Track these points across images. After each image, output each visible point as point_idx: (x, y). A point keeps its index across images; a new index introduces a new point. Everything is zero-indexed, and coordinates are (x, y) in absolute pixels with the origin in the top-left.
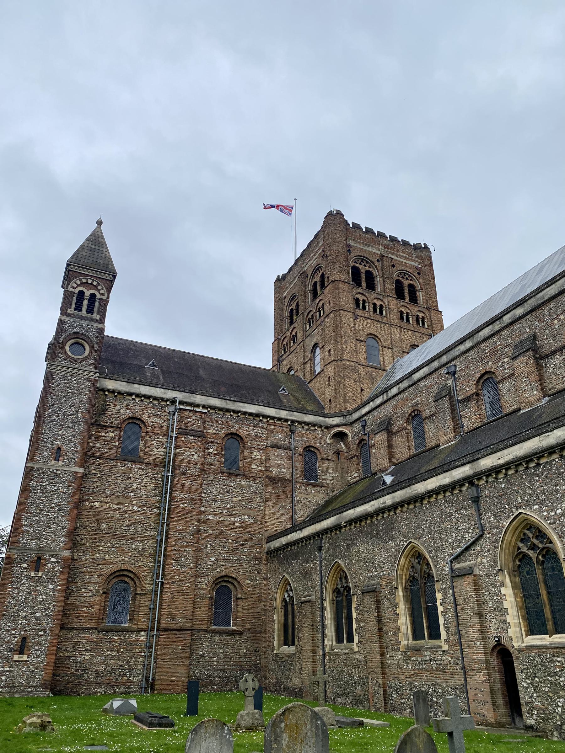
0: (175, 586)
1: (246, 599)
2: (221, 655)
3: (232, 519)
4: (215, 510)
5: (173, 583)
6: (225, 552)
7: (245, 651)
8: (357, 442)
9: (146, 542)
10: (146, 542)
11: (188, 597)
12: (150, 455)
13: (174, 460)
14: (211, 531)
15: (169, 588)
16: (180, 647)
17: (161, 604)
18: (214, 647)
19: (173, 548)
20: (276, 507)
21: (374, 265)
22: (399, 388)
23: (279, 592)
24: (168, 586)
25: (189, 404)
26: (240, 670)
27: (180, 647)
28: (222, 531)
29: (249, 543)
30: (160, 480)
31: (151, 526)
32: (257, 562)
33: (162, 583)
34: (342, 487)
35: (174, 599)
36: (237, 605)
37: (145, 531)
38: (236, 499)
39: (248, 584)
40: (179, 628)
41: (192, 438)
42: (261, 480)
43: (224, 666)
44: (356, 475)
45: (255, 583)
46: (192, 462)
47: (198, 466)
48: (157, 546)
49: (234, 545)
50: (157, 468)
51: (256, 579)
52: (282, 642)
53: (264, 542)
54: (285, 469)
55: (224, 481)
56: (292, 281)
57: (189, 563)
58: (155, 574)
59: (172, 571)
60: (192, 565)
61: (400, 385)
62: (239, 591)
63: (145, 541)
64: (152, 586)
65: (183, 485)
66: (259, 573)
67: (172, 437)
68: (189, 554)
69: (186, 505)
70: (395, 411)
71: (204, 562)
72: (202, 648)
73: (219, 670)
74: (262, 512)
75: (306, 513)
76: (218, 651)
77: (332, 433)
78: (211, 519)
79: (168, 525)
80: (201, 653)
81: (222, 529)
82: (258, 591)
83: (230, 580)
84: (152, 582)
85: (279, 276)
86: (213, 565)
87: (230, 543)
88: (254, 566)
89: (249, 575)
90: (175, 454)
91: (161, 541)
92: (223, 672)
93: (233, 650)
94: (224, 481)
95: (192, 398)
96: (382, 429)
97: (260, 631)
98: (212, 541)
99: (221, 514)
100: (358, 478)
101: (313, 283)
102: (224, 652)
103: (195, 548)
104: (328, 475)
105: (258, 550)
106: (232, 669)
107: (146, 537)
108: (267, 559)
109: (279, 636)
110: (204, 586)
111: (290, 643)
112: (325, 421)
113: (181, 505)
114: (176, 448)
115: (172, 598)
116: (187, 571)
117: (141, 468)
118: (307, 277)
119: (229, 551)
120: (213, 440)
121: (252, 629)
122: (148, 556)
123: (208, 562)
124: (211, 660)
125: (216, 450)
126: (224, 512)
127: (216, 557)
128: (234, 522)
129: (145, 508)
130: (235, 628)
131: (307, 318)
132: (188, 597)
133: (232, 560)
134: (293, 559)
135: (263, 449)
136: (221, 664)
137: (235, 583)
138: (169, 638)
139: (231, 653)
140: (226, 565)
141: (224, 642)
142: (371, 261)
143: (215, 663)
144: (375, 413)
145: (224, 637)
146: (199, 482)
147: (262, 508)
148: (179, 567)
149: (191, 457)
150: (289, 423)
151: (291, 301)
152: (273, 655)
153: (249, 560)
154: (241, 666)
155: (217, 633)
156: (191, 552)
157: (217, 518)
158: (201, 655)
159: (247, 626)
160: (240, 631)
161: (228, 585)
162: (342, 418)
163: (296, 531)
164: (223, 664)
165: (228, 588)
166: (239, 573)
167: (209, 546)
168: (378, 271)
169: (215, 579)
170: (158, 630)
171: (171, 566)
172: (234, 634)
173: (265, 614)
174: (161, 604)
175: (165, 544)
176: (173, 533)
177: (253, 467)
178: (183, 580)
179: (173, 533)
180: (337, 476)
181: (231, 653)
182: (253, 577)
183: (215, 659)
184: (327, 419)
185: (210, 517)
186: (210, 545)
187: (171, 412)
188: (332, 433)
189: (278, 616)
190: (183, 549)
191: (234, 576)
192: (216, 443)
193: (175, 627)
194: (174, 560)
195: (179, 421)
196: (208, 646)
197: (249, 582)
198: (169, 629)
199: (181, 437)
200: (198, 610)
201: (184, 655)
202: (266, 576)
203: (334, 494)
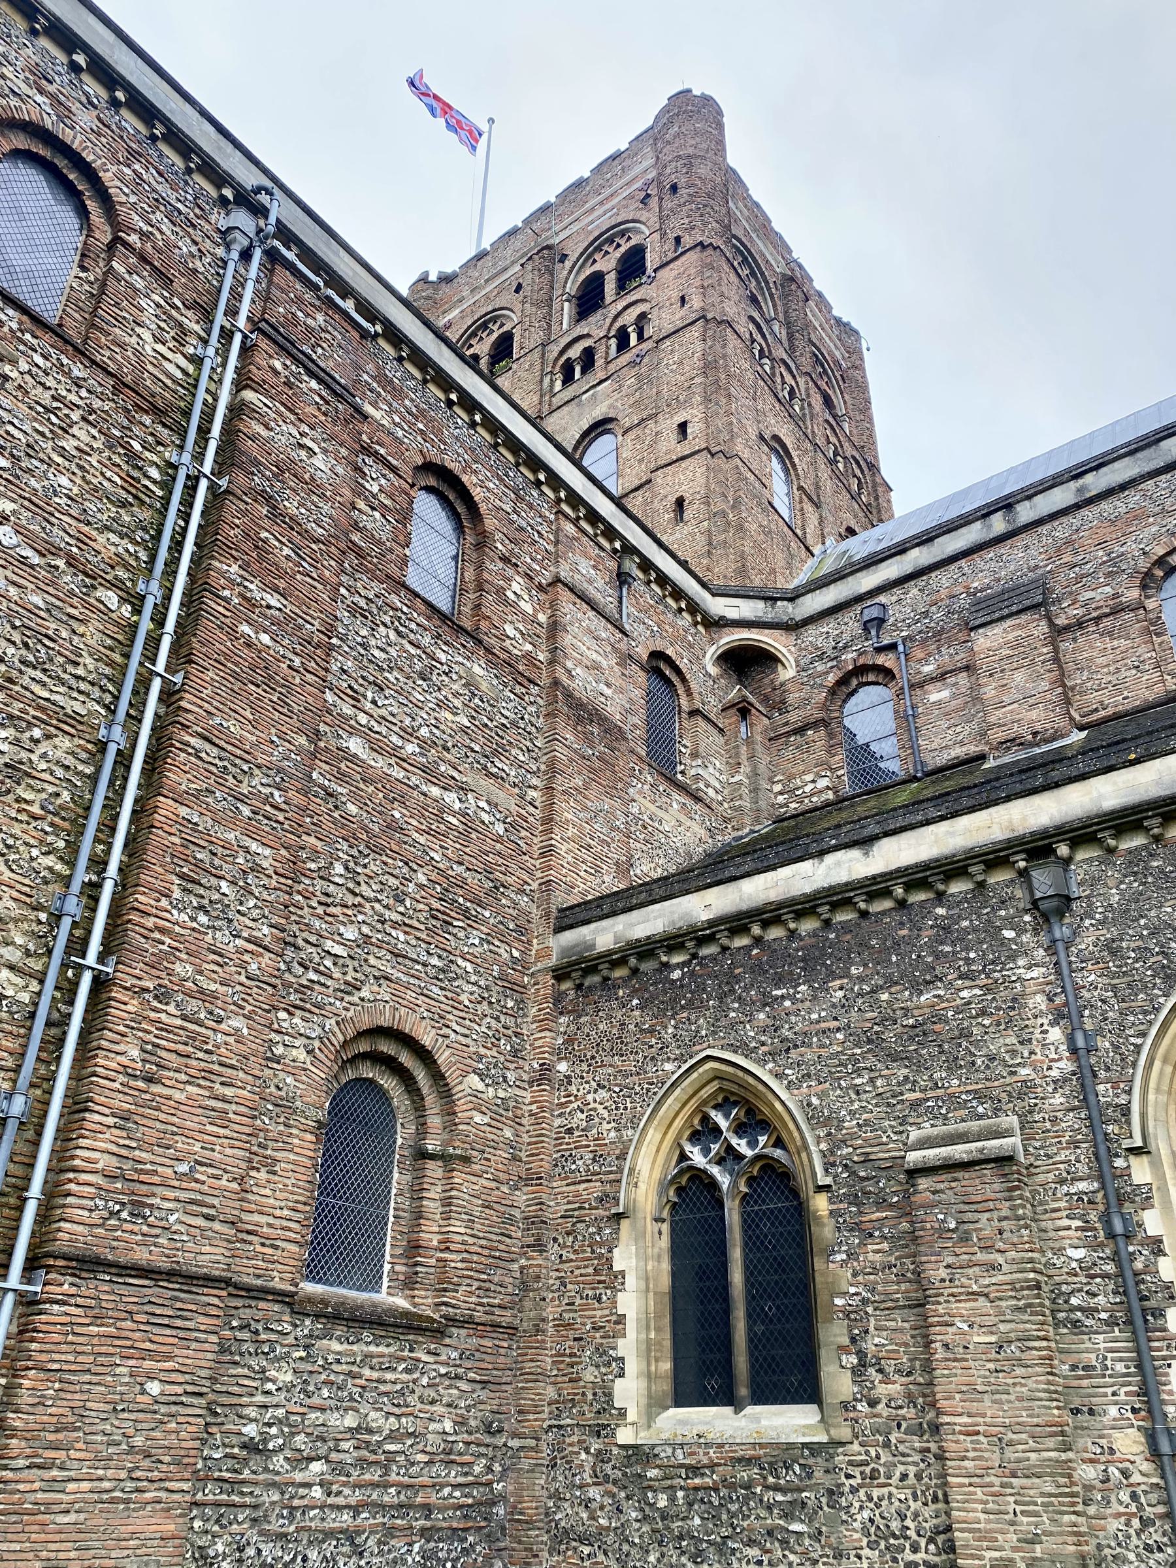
0: (169, 1015)
1: (466, 1160)
2: (345, 1445)
3: (435, 791)
4: (373, 723)
5: (163, 996)
6: (399, 918)
7: (448, 1426)
8: (831, 679)
9: (37, 733)
10: (37, 733)
11: (229, 1092)
12: (122, 346)
13: (229, 431)
14: (352, 809)
15: (139, 1018)
16: (154, 1388)
17: (77, 1106)
18: (316, 1400)
19: (184, 811)
20: (585, 808)
21: (769, 289)
22: (1080, 490)
23: (653, 1135)
24: (133, 1006)
25: (307, 254)
26: (423, 1531)
27: (154, 1388)
28: (393, 827)
29: (487, 914)
30: (154, 473)
31: (76, 664)
32: (510, 1004)
33: (100, 984)
34: (757, 820)
35: (156, 1089)
36: (416, 1191)
37: (38, 674)
38: (450, 717)
39: (476, 1094)
40: (163, 1264)
41: (314, 384)
42: (534, 690)
43: (356, 1510)
44: (823, 783)
45: (502, 1094)
46: (307, 476)
47: (326, 508)
48: (94, 779)
49: (436, 905)
50: (147, 420)
51: (505, 1080)
52: (666, 1386)
53: (538, 926)
54: (608, 685)
55: (413, 626)
56: (487, 281)
57: (256, 913)
58: (66, 922)
59: (162, 931)
60: (266, 930)
61: (1089, 478)
62: (435, 1121)
63: (30, 725)
64: (34, 986)
65: (261, 547)
66: (515, 1053)
67: (227, 335)
68: (257, 869)
69: (265, 638)
70: (1067, 558)
71: (313, 939)
72: (259, 1398)
73: (329, 1534)
74: (531, 809)
75: (659, 870)
76: (333, 1419)
77: (723, 642)
78: (355, 756)
79: (169, 696)
80: (251, 1430)
81: (397, 815)
82: (508, 1133)
83: (406, 1059)
84: (36, 965)
85: (427, 274)
86: (349, 962)
87: (421, 886)
88: (497, 1019)
89: (483, 1051)
90: (237, 410)
91: (124, 760)
92: (346, 1549)
93: (398, 1416)
94: (413, 626)
95: (321, 245)
96: (997, 615)
97: (512, 1331)
98: (354, 852)
99: (394, 752)
100: (830, 795)
101: (582, 277)
102: (358, 1429)
103: (283, 852)
104: (711, 770)
105: (516, 954)
106: (390, 1532)
107: (43, 709)
108: (558, 998)
109: (648, 1351)
110: (301, 1055)
111: (743, 1391)
112: (704, 600)
113: (245, 628)
114: (242, 382)
115: (149, 1080)
116: (241, 952)
117: (68, 374)
118: (562, 261)
119: (416, 924)
120: (382, 451)
121: (479, 1316)
122: (36, 809)
123: (329, 945)
124: (298, 1477)
125: (390, 496)
126: (411, 748)
127: (366, 930)
128: (443, 809)
129: (61, 563)
130: (401, 1302)
131: (557, 359)
132: (229, 1092)
133: (425, 965)
134: (779, 981)
135: (540, 588)
136: (340, 1501)
137: (421, 1076)
138: (97, 1319)
139: (392, 1437)
140: (397, 981)
141: (367, 1372)
142: (762, 274)
143: (317, 1492)
144: (942, 580)
145: (368, 1346)
146: (327, 573)
147: (532, 794)
148: (203, 919)
149: (303, 453)
150: (617, 545)
151: (474, 334)
152: (601, 1457)
153: (482, 983)
154: (427, 1509)
155: (335, 1318)
156: (265, 864)
157: (379, 763)
158: (251, 1447)
159: (463, 1299)
160: (430, 1319)
161: (388, 1083)
162: (761, 604)
163: (822, 853)
164: (353, 1501)
165: (383, 1095)
166: (445, 1031)
167: (339, 868)
168: (775, 306)
169: (350, 1033)
170: (32, 1265)
171: (164, 903)
172: (410, 1328)
173: (540, 1247)
174: (77, 1106)
175: (140, 786)
176: (193, 741)
177: (510, 630)
178: (214, 995)
179: (193, 741)
180: (739, 783)
181: (392, 1437)
182: (496, 1066)
183: (317, 1467)
184: (706, 595)
185: (355, 745)
186: (347, 868)
187: (237, 235)
188: (723, 642)
189: (643, 1256)
190: (231, 836)
191: (427, 1040)
192: (393, 469)
193: (141, 1256)
194: (182, 876)
195: (265, 297)
196: (290, 1388)
197: (480, 1086)
198: (106, 1265)
199: (271, 352)
200: (263, 1175)
201: (172, 1440)
202: (544, 1075)
203: (728, 839)
